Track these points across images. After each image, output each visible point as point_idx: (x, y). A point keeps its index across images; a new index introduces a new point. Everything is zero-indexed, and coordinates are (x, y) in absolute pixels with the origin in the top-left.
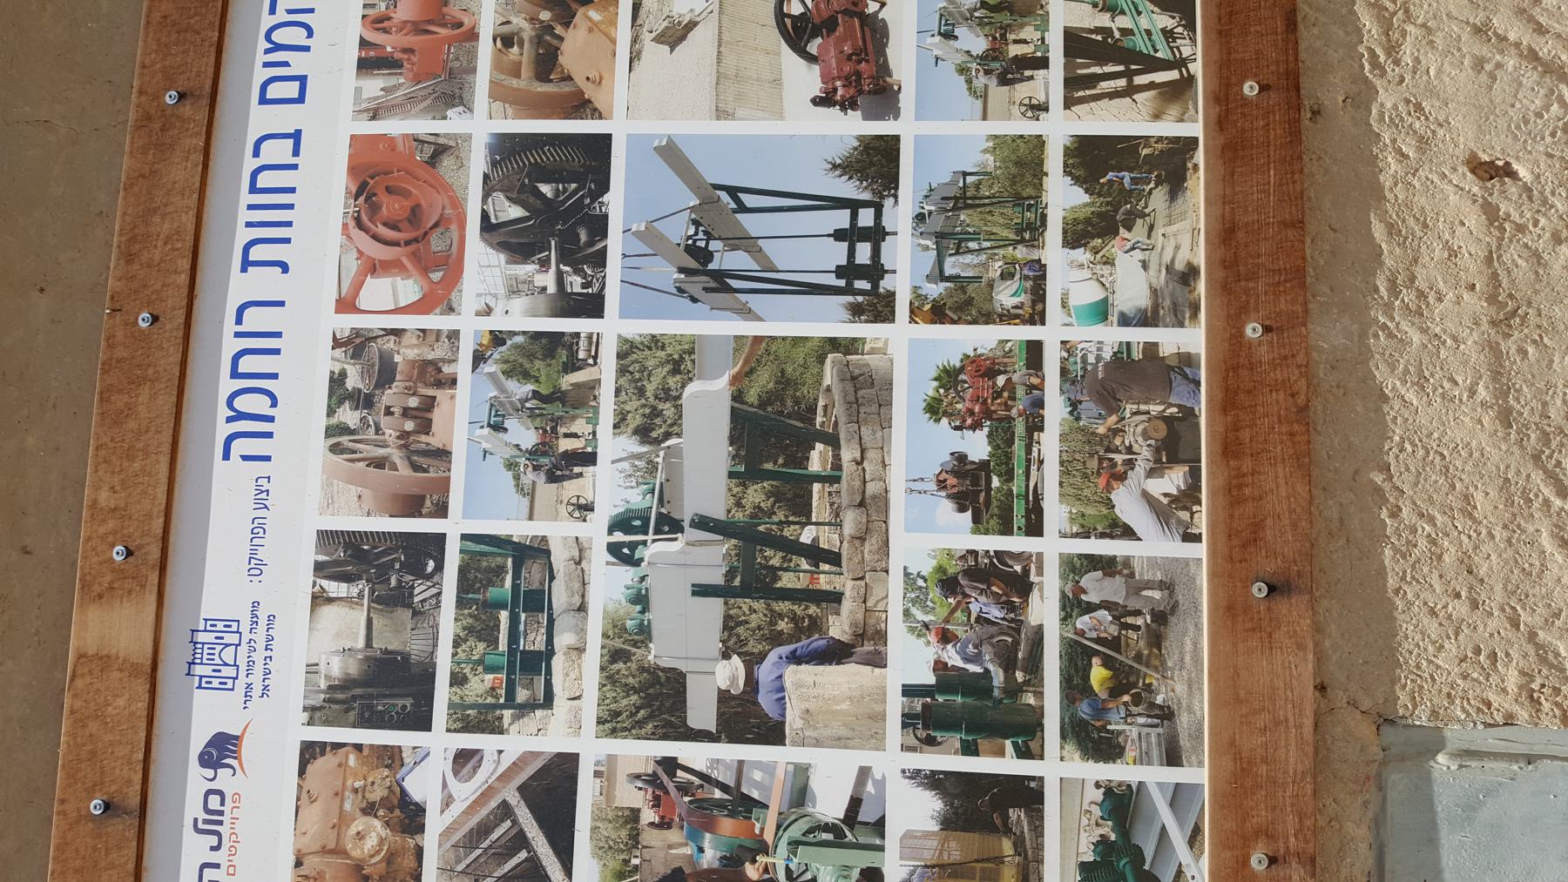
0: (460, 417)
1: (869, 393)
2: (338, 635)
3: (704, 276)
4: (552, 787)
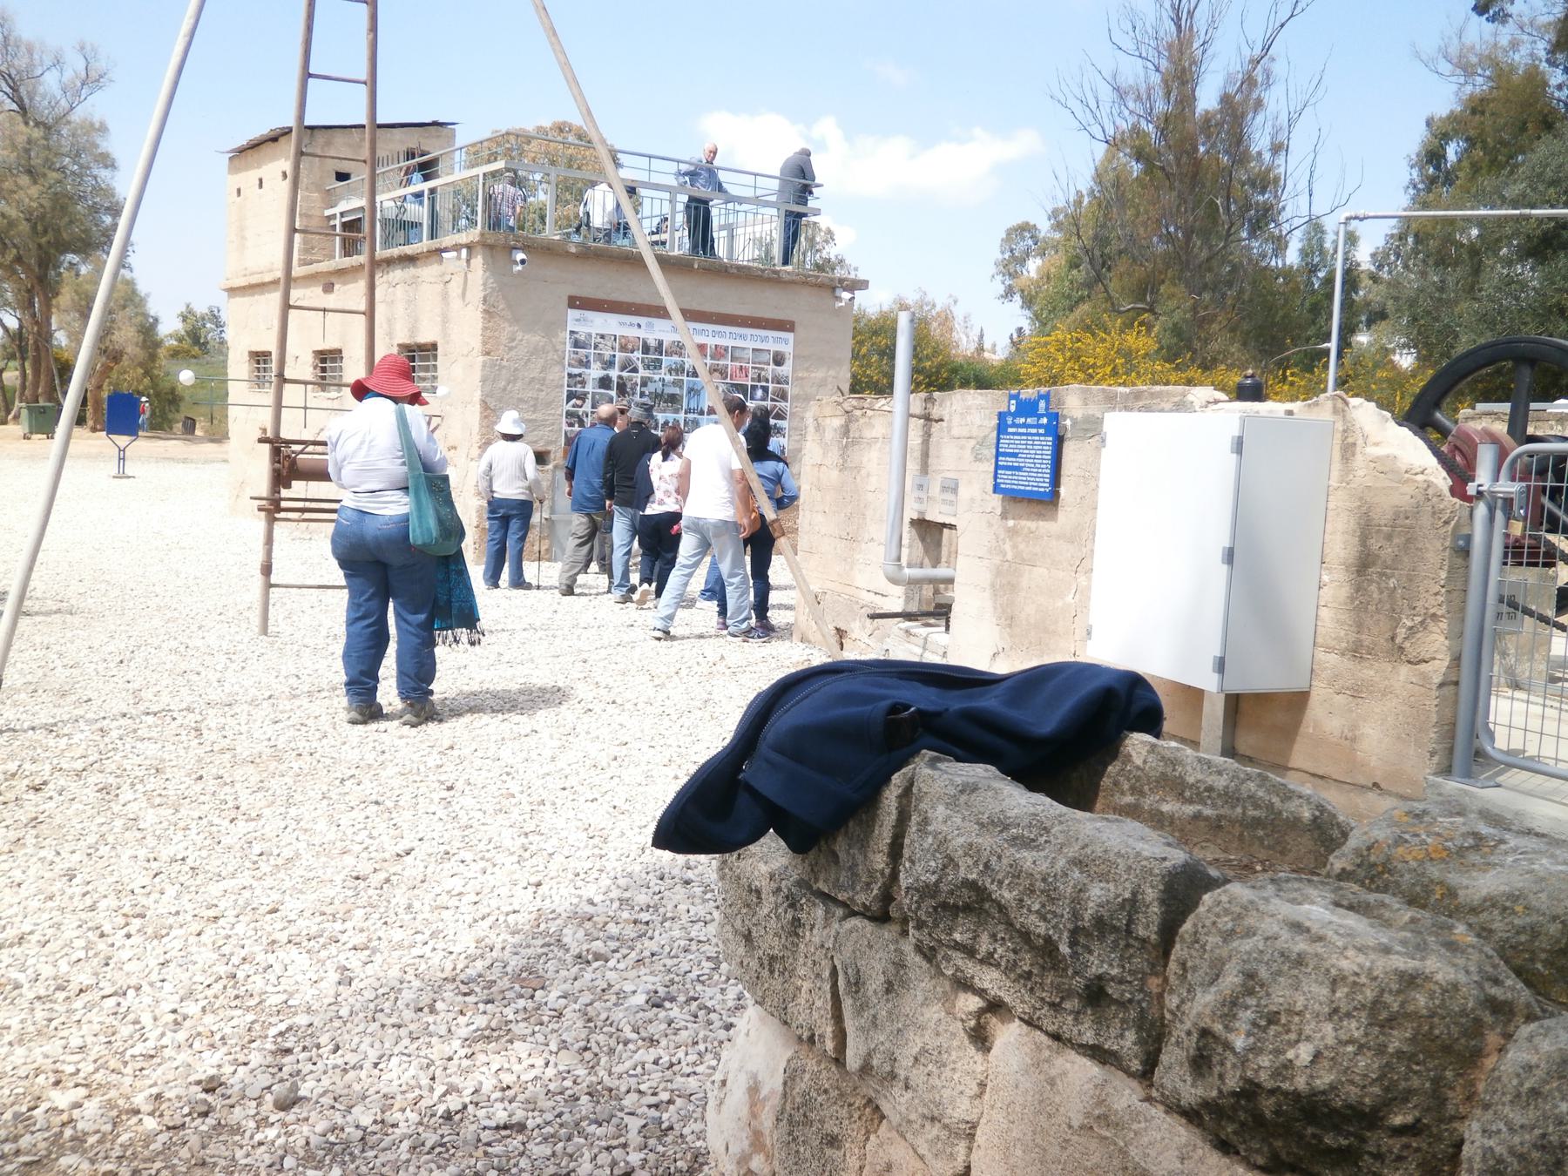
0: (676, 358)
1: (677, 411)
2: (652, 343)
3: (690, 390)
4: (635, 370)
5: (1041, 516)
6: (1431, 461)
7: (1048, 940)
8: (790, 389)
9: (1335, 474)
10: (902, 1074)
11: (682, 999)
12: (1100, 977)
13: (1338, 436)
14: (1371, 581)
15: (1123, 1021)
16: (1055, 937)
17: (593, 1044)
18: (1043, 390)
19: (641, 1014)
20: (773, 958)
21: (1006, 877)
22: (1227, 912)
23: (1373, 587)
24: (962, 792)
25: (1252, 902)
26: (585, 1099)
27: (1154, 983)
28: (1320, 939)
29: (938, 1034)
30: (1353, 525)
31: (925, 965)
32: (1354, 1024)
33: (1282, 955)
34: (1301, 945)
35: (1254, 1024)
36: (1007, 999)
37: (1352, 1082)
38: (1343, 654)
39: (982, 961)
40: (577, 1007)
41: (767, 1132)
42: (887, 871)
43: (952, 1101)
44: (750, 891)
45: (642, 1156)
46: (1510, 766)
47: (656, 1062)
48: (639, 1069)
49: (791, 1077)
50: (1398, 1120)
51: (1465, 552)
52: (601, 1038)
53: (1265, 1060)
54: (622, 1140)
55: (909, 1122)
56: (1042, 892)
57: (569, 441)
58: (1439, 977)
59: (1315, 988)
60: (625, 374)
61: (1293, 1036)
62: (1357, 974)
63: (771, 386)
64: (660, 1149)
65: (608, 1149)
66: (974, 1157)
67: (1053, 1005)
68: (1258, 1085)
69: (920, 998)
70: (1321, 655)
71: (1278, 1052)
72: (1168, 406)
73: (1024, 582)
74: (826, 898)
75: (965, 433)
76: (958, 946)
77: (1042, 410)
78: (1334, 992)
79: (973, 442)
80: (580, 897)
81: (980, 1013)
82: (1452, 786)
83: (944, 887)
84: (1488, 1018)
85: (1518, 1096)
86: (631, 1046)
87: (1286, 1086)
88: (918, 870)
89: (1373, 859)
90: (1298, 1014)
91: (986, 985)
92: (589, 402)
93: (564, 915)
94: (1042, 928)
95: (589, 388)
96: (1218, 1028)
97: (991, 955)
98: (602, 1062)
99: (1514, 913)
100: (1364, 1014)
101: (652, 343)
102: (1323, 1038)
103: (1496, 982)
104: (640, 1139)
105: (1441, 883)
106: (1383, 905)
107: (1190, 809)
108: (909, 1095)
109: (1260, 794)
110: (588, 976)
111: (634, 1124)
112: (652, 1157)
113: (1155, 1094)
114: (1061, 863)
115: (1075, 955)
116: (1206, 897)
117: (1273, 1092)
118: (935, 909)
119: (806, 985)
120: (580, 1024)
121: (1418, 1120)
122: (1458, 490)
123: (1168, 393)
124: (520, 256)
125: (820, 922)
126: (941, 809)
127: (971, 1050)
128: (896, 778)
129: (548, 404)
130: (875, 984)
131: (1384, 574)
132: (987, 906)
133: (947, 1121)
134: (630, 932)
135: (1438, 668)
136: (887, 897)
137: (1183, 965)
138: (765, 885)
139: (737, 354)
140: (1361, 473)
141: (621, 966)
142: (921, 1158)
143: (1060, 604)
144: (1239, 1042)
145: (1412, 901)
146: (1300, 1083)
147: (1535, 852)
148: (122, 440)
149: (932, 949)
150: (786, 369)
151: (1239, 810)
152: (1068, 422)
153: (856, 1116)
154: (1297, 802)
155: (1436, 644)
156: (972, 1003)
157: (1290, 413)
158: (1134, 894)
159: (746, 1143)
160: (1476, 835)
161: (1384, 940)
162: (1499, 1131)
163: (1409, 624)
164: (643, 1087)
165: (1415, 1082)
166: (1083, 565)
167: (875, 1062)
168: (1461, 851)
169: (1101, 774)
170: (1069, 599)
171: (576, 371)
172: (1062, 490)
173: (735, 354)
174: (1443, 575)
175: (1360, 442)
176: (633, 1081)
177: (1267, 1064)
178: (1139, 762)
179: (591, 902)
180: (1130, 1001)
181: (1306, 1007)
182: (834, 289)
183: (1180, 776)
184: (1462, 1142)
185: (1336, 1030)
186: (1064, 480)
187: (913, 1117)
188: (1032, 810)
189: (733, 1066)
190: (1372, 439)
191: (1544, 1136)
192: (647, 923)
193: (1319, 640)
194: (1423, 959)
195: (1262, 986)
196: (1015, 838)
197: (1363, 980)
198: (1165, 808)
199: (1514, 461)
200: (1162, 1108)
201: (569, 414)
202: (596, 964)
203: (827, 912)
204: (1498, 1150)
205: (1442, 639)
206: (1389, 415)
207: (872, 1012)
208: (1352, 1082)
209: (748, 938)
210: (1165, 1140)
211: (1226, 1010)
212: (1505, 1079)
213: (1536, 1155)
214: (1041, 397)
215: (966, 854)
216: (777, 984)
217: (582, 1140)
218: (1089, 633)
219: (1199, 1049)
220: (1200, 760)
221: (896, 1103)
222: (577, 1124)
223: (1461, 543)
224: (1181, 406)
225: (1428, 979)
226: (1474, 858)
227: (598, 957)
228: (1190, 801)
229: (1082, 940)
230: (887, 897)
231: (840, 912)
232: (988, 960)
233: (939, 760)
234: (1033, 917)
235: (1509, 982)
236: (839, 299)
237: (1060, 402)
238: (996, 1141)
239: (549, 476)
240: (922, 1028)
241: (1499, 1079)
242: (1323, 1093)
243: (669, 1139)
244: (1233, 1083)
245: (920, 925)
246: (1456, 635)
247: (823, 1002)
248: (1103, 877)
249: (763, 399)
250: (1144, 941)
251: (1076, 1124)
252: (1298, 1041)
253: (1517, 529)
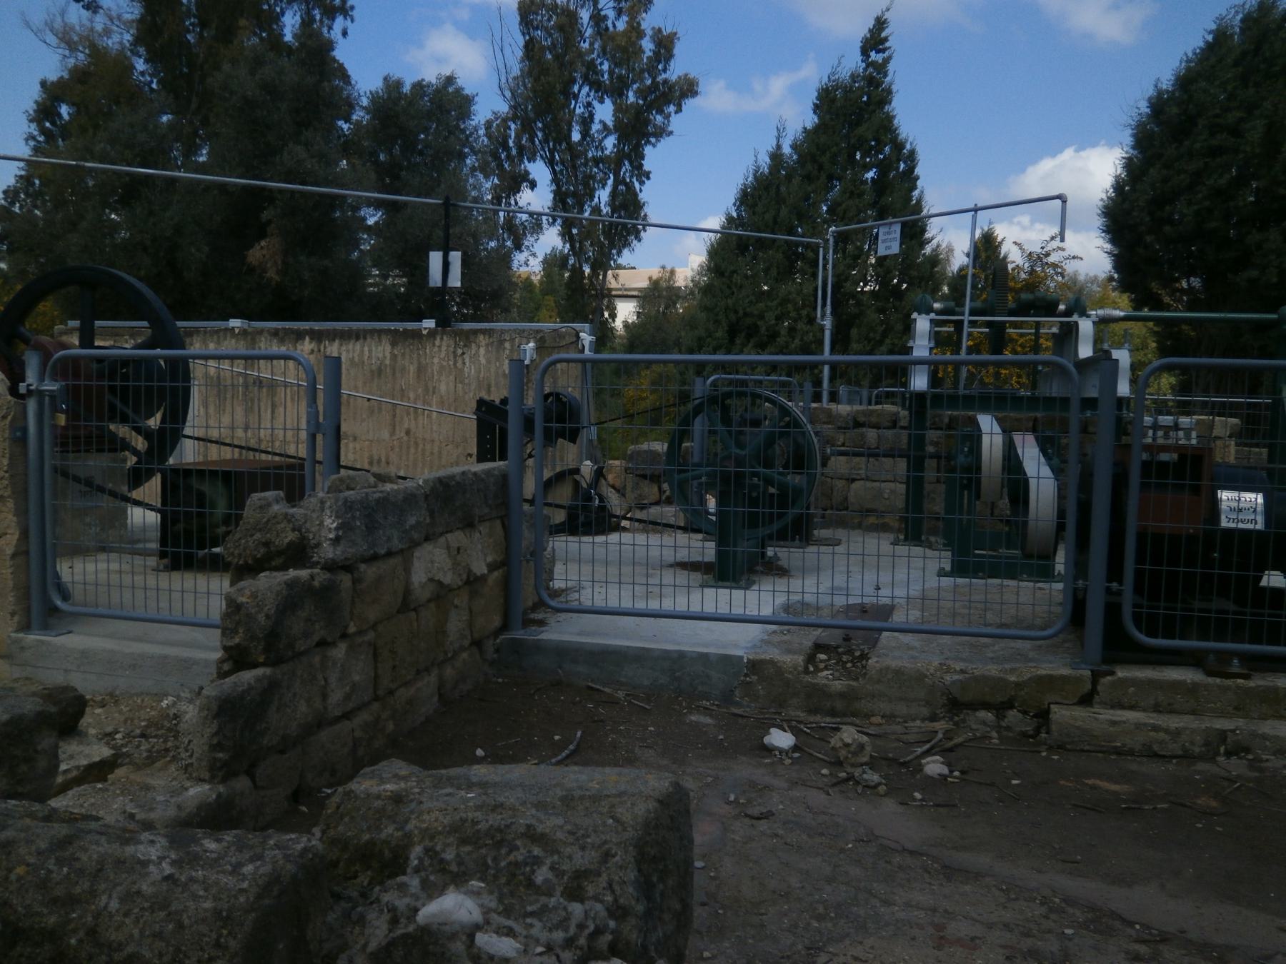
82: (32, 637)
122: (13, 391)
174: (5, 462)
199: (55, 363)
205: (10, 516)
223: (18, 434)
246: (22, 512)
253: (62, 420)
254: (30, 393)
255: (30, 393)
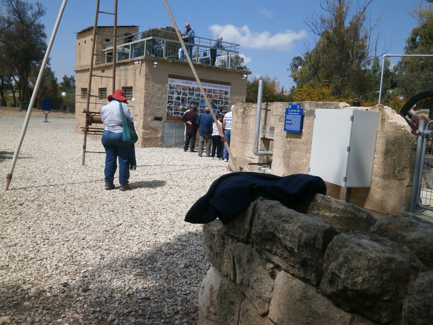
0: (198, 92)
2: (191, 88)
3: (202, 101)
4: (187, 95)
5: (297, 137)
6: (406, 124)
7: (292, 248)
8: (229, 102)
9: (379, 127)
10: (251, 285)
11: (194, 266)
12: (305, 259)
13: (380, 116)
14: (389, 157)
15: (311, 271)
16: (294, 247)
17: (169, 277)
18: (299, 102)
19: (182, 270)
20: (217, 253)
21: (281, 231)
22: (340, 241)
23: (389, 159)
24: (269, 208)
25: (347, 238)
26: (166, 292)
27: (320, 261)
28: (366, 248)
29: (261, 274)
30: (384, 141)
31: (258, 255)
32: (374, 272)
33: (355, 252)
34: (360, 250)
35: (347, 271)
36: (280, 265)
37: (373, 288)
38: (380, 177)
39: (274, 254)
40: (165, 267)
41: (215, 301)
42: (249, 229)
43: (265, 292)
44: (212, 235)
45: (181, 308)
46: (426, 209)
47: (186, 283)
48: (181, 284)
49: (221, 286)
50: (385, 298)
51: (415, 150)
52: (171, 276)
53: (349, 281)
54: (176, 303)
55: (253, 298)
56: (290, 235)
57: (168, 114)
58: (398, 259)
59: (364, 262)
60: (184, 96)
61: (357, 275)
62: (375, 258)
63: (224, 100)
64: (186, 306)
65: (172, 305)
66: (270, 308)
67: (292, 266)
68: (347, 288)
69: (257, 264)
70: (374, 177)
71: (353, 279)
72: (333, 107)
73: (292, 155)
74: (232, 237)
75: (277, 114)
76: (267, 250)
77: (298, 108)
78: (369, 263)
79: (279, 117)
80: (167, 238)
81: (273, 268)
83: (264, 234)
84: (411, 271)
85: (418, 292)
86: (179, 278)
87: (355, 288)
88: (257, 229)
89: (382, 228)
90: (359, 269)
91: (275, 261)
92: (174, 104)
93: (162, 243)
94: (290, 245)
95: (174, 100)
96: (337, 272)
97: (276, 252)
98: (171, 282)
99: (421, 243)
100: (377, 269)
101: (191, 88)
102: (365, 275)
103: (414, 261)
104: (181, 303)
105: (401, 235)
106: (384, 240)
107: (333, 215)
108: (253, 291)
109: (352, 211)
110: (168, 259)
111: (179, 299)
112: (184, 308)
113: (319, 291)
114: (296, 227)
115: (299, 252)
116: (335, 237)
117: (351, 290)
118: (261, 240)
119: (226, 261)
120: (166, 272)
121: (391, 299)
123: (333, 104)
124: (156, 63)
125: (230, 243)
126: (264, 212)
127: (270, 279)
128: (252, 204)
129: (163, 104)
130: (245, 260)
131: (392, 155)
132: (275, 239)
133: (263, 298)
134: (180, 247)
135: (406, 182)
136: (248, 236)
137: (328, 255)
138: (216, 233)
139: (215, 91)
140: (386, 127)
141: (178, 257)
142: (256, 308)
143: (302, 162)
144: (342, 276)
145: (392, 239)
146: (359, 287)
147: (427, 227)
148: (47, 112)
149: (260, 251)
150: (228, 96)
151: (346, 215)
152: (305, 111)
153: (239, 296)
154: (362, 213)
155: (407, 174)
156: (271, 266)
157: (367, 110)
158: (315, 236)
159: (209, 304)
160: (411, 223)
161: (384, 249)
162: (413, 301)
163: (399, 169)
164: (182, 289)
165: (391, 288)
166: (308, 151)
167: (244, 282)
168: (407, 227)
169: (309, 205)
170: (304, 160)
171: (170, 95)
172: (303, 130)
173: (214, 91)
174: (409, 156)
175: (387, 118)
176: (180, 287)
177: (350, 282)
178: (319, 201)
179: (170, 239)
180: (314, 265)
181: (361, 267)
182: (242, 74)
183: (331, 206)
184: (403, 304)
185: (369, 273)
186: (304, 127)
187: (254, 297)
188: (288, 213)
189: (206, 282)
190: (390, 118)
191: (425, 303)
192: (185, 245)
193: (373, 173)
194: (394, 254)
195: (349, 261)
196: (283, 220)
197: (377, 260)
198: (326, 214)
200: (321, 295)
201: (168, 107)
202: (171, 256)
203: (232, 241)
204: (412, 306)
206: (395, 111)
207: (244, 268)
208: (373, 288)
209: (211, 248)
210: (322, 304)
211: (339, 267)
212: (415, 287)
213: (423, 308)
214: (298, 104)
215: (270, 225)
216: (218, 260)
217: (165, 303)
218: (309, 170)
219: (331, 278)
220: (336, 201)
221: (249, 293)
222: (164, 299)
224: (337, 107)
225: (395, 260)
226: (410, 228)
227: (171, 254)
228: (333, 212)
229: (301, 248)
230: (248, 236)
231: (236, 241)
232: (275, 254)
233: (264, 199)
234: (288, 242)
235: (418, 262)
236: (244, 77)
237: (303, 106)
238: (276, 303)
239: (162, 124)
240: (257, 272)
241: (413, 287)
242: (365, 290)
243: (189, 303)
244: (340, 287)
245: (257, 244)
246: (412, 172)
247: (230, 265)
248: (307, 231)
249: (222, 104)
250: (318, 249)
251: (298, 299)
252: (358, 276)
254: (420, 134)
255: (420, 133)
